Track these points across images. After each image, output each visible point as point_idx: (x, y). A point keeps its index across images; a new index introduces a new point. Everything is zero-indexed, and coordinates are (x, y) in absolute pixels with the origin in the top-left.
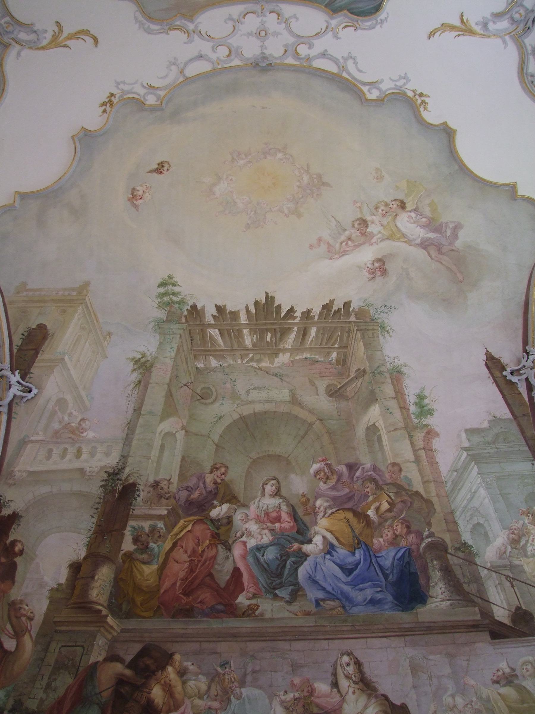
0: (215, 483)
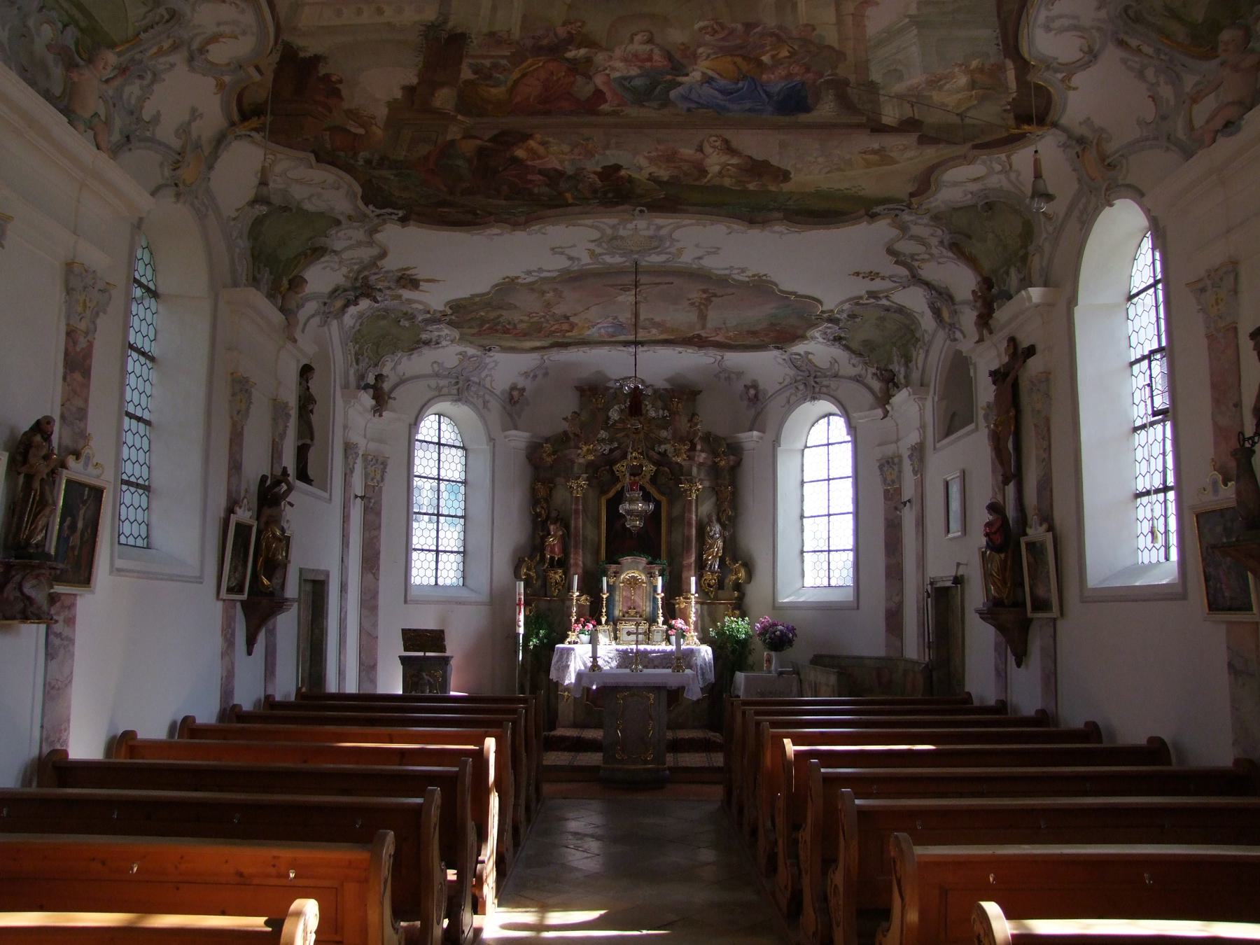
0: (569, 33)
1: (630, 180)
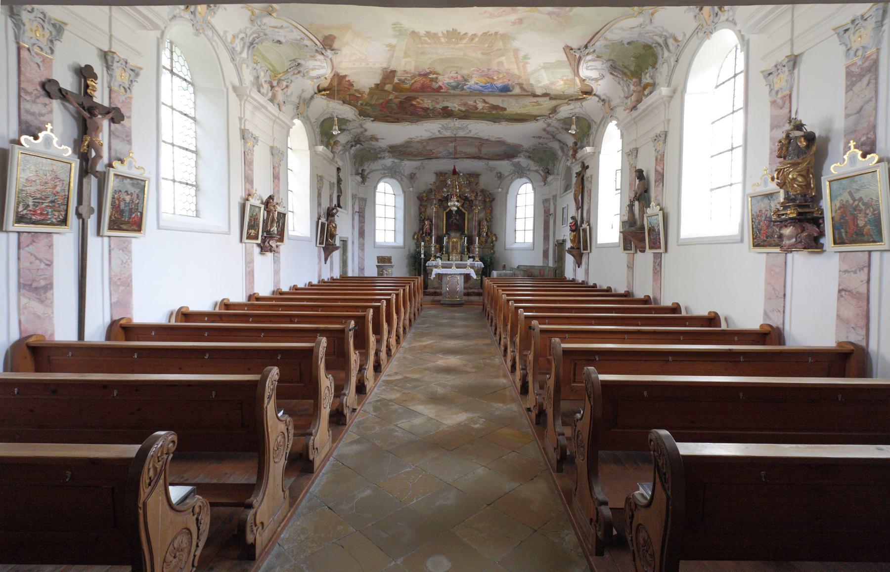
1: (452, 110)
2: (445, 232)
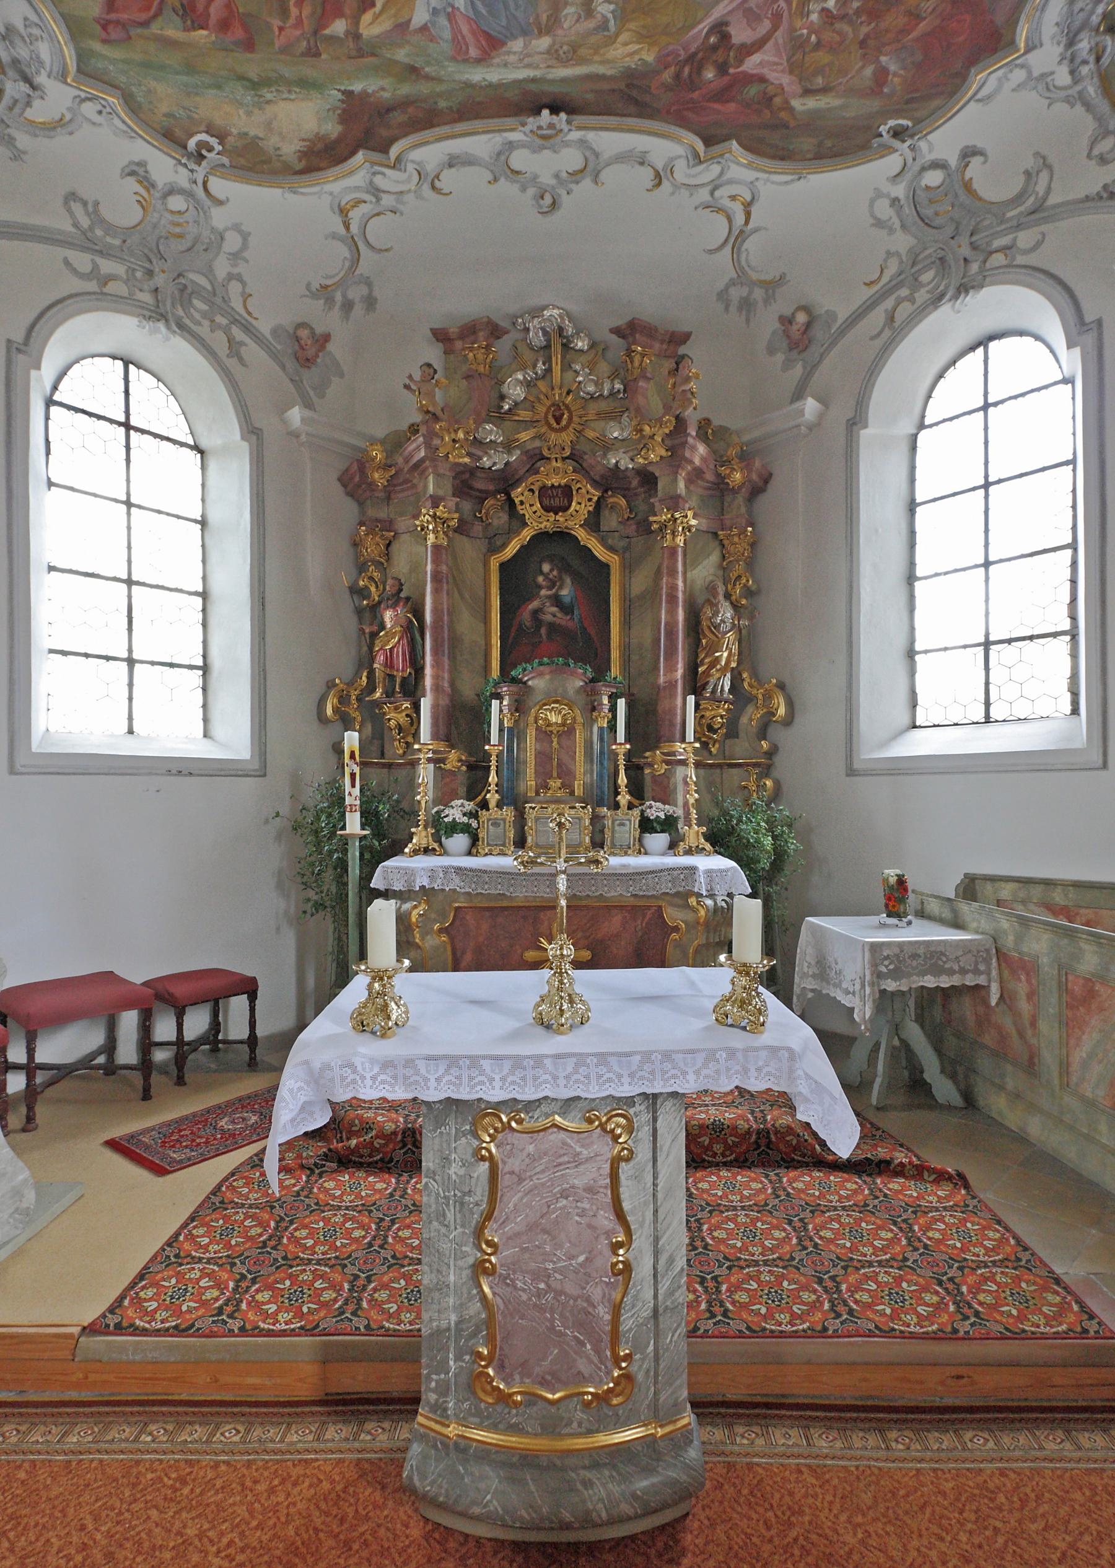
2: (495, 672)
